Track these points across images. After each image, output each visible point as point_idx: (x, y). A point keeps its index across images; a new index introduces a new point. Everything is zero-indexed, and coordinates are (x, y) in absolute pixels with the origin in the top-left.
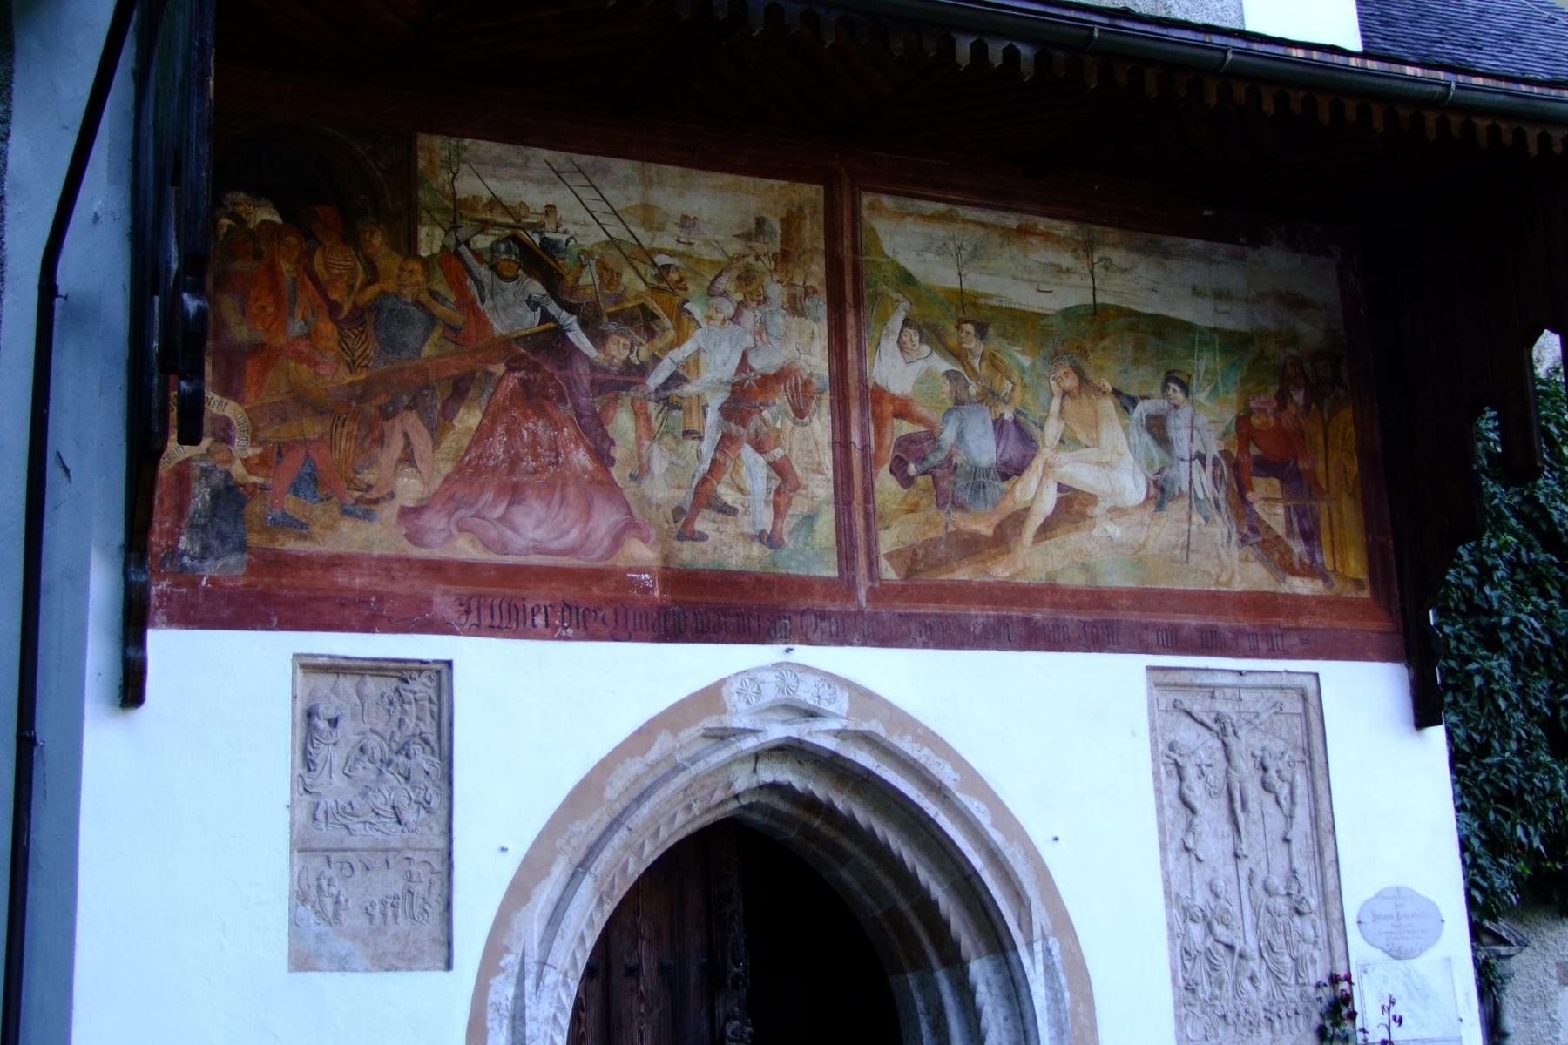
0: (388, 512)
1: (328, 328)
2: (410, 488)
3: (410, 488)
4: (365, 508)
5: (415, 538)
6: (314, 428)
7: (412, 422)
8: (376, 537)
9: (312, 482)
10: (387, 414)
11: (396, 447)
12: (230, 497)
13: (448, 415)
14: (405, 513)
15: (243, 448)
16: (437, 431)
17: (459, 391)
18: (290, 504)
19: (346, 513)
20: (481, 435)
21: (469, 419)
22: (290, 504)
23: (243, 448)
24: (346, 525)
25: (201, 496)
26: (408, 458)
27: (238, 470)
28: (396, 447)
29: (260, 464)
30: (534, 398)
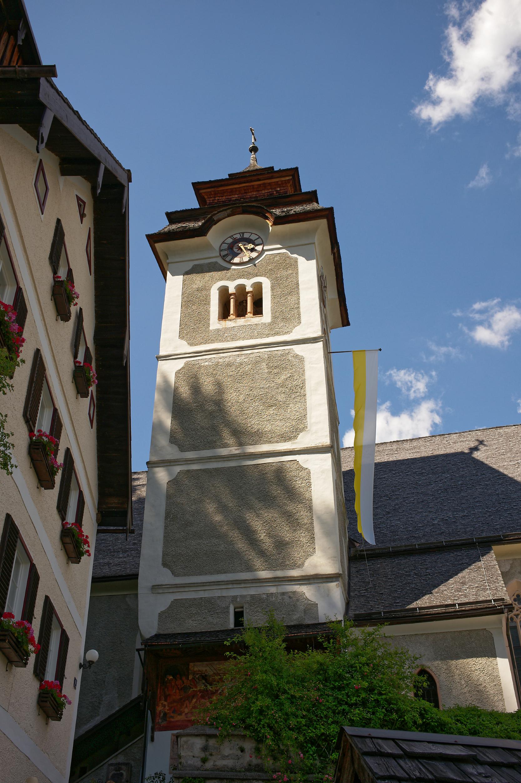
0: (184, 714)
1: (178, 691)
2: (186, 710)
3: (186, 710)
4: (180, 714)
5: (187, 717)
6: (175, 704)
7: (187, 702)
8: (182, 717)
9: (174, 712)
10: (184, 701)
11: (185, 705)
12: (165, 714)
13: (192, 700)
14: (186, 714)
15: (167, 708)
16: (190, 703)
17: (193, 697)
18: (172, 715)
19: (178, 715)
20: (196, 702)
21: (194, 700)
22: (172, 715)
23: (167, 708)
24: (178, 716)
25: (162, 714)
26: (186, 707)
27: (166, 711)
28: (185, 705)
29: (169, 710)
30: (203, 697)
